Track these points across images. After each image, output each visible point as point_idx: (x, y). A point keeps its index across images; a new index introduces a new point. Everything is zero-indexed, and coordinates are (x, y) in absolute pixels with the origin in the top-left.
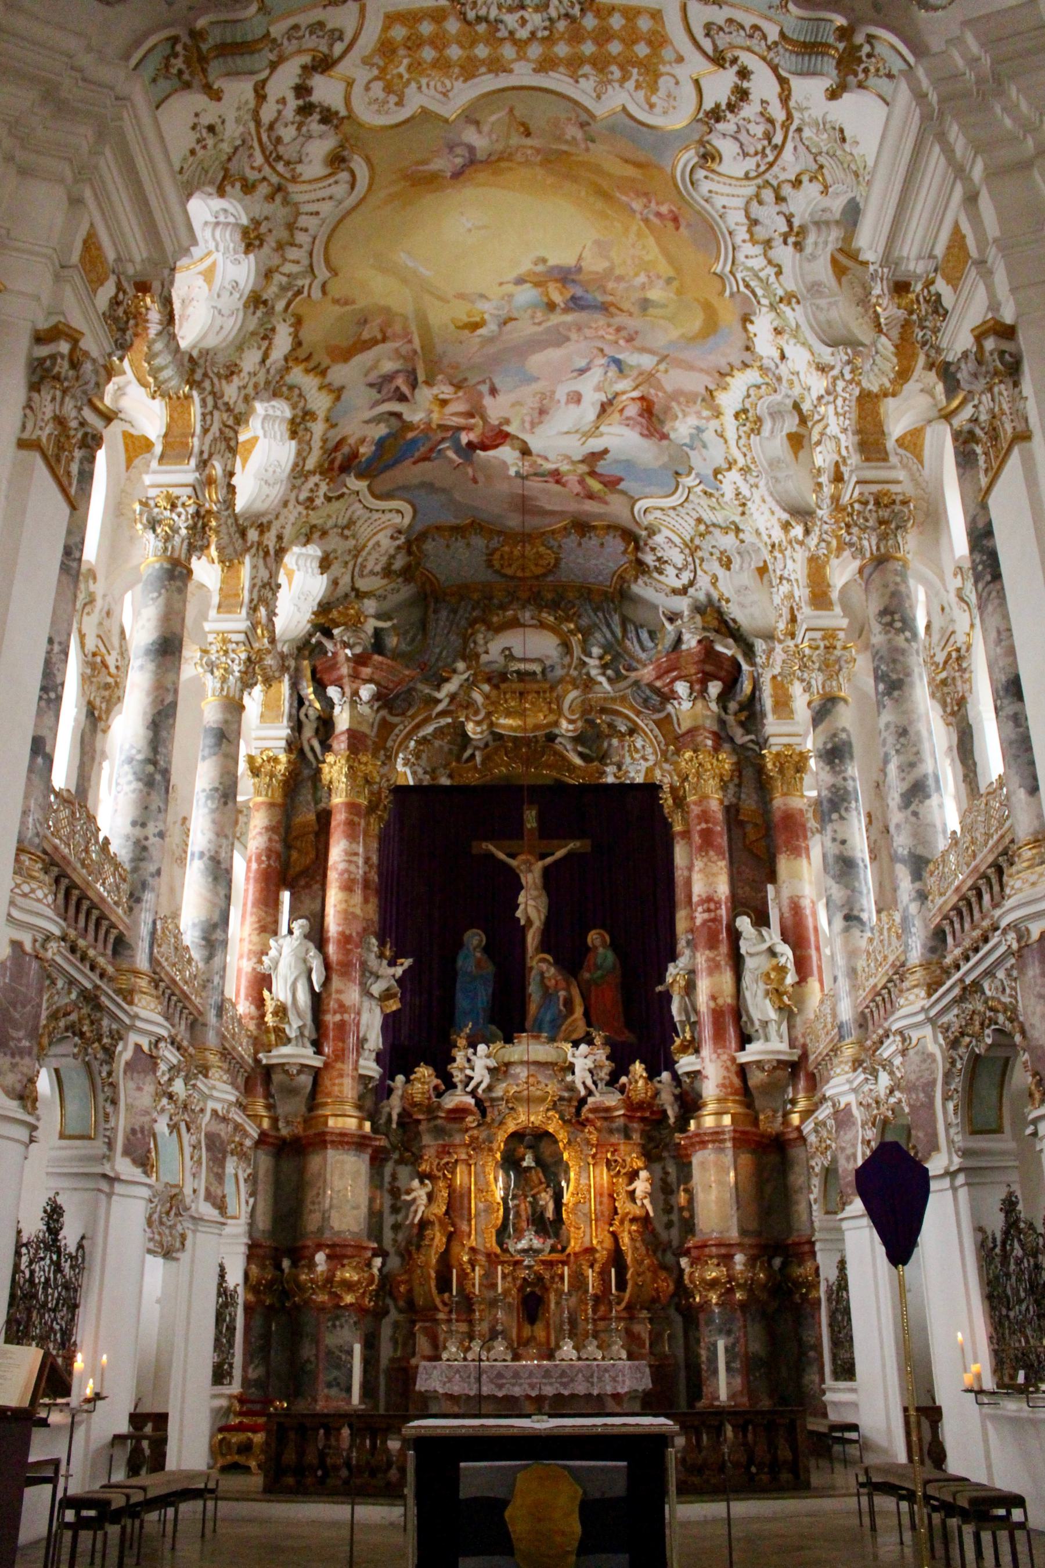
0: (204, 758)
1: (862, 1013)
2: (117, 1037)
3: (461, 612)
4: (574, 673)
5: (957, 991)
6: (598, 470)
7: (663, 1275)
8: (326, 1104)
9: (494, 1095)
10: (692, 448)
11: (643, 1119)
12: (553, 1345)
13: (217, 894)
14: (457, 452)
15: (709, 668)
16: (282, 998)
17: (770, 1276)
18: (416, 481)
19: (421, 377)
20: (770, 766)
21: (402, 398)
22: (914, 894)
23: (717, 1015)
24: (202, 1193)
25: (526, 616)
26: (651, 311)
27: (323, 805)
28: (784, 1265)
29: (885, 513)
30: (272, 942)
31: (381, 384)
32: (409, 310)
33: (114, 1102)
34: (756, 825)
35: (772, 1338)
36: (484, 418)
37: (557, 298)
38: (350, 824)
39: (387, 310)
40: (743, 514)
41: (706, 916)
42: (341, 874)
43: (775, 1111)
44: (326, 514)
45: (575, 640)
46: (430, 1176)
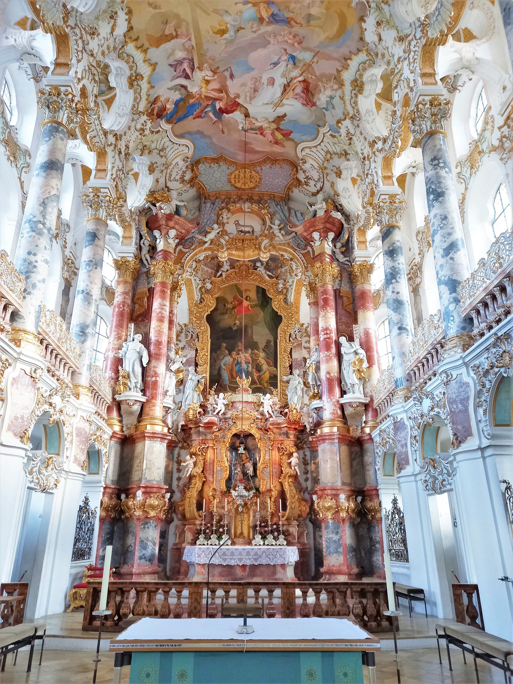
0: (86, 246)
1: (409, 373)
3: (216, 204)
4: (266, 232)
6: (281, 127)
7: (304, 503)
9: (227, 416)
11: (295, 429)
12: (251, 537)
15: (328, 225)
17: (357, 506)
18: (195, 130)
19: (196, 65)
20: (356, 270)
21: (187, 77)
23: (330, 381)
24: (72, 459)
25: (247, 206)
26: (312, 22)
28: (363, 501)
29: (435, 110)
31: (175, 65)
32: (189, 18)
35: (358, 537)
37: (265, 15)
39: (177, 16)
40: (350, 144)
41: (325, 336)
43: (357, 427)
46: (195, 454)
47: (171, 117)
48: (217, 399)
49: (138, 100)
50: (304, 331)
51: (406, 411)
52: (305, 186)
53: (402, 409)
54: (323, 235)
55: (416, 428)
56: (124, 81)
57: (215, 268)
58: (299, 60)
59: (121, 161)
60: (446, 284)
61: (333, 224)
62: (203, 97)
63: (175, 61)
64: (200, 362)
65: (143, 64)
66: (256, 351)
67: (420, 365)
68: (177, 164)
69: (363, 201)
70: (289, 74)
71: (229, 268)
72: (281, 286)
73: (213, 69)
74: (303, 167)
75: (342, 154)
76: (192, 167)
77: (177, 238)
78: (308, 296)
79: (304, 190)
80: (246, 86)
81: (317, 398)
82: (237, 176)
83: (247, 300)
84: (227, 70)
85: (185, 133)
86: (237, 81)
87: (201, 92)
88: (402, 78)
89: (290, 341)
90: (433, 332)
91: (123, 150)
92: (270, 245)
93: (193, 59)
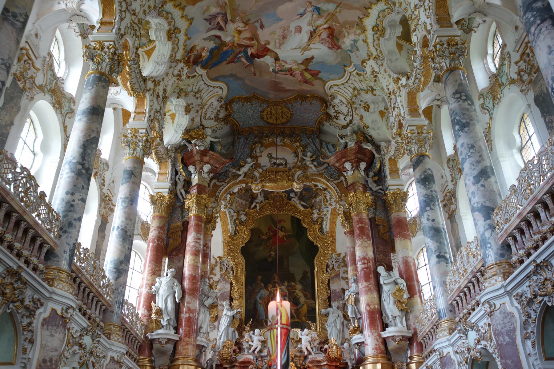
0: (122, 184)
1: (451, 304)
2: (38, 303)
3: (249, 139)
4: (299, 164)
5: (532, 267)
6: (309, 68)
8: (179, 359)
9: (263, 354)
10: (352, 52)
13: (124, 247)
14: (246, 59)
15: (359, 156)
16: (160, 306)
19: (229, 18)
20: (390, 198)
21: (221, 29)
22: (487, 227)
23: (371, 313)
25: (278, 140)
27: (185, 219)
29: (453, 50)
30: (157, 280)
31: (211, 19)
33: (32, 342)
34: (384, 226)
36: (258, 41)
38: (198, 226)
40: (375, 81)
41: (363, 266)
42: (192, 248)
43: (402, 363)
44: (186, 84)
45: (299, 150)
47: (206, 63)
48: (253, 336)
49: (176, 50)
50: (341, 260)
51: (452, 345)
52: (335, 120)
53: (447, 343)
54: (355, 165)
55: (464, 363)
56: (163, 35)
57: (250, 200)
58: (324, 11)
59: (158, 104)
60: (479, 210)
61: (365, 154)
62: (236, 45)
63: (210, 15)
64: (235, 296)
65: (180, 20)
66: (293, 283)
67: (462, 294)
68: (212, 104)
69: (392, 133)
70: (315, 22)
71: (263, 199)
72: (316, 215)
73: (244, 21)
74: (332, 103)
75: (368, 90)
76: (226, 106)
77: (211, 173)
78: (343, 225)
79: (334, 124)
80: (275, 34)
81: (358, 332)
82: (269, 113)
83: (282, 230)
84: (257, 21)
85: (219, 77)
86: (267, 30)
87: (234, 41)
88: (420, 22)
89: (327, 271)
90: (472, 259)
91: (161, 94)
92: (303, 176)
93: (226, 13)
